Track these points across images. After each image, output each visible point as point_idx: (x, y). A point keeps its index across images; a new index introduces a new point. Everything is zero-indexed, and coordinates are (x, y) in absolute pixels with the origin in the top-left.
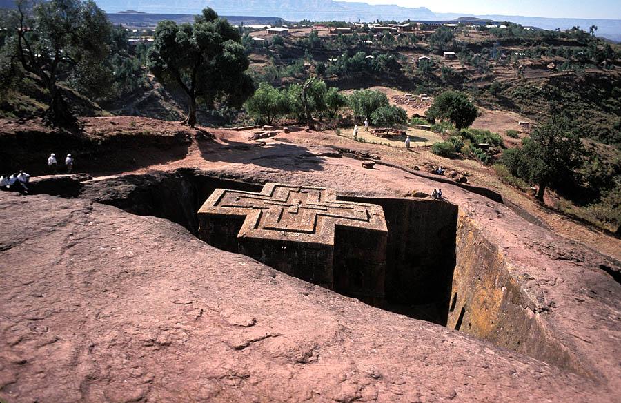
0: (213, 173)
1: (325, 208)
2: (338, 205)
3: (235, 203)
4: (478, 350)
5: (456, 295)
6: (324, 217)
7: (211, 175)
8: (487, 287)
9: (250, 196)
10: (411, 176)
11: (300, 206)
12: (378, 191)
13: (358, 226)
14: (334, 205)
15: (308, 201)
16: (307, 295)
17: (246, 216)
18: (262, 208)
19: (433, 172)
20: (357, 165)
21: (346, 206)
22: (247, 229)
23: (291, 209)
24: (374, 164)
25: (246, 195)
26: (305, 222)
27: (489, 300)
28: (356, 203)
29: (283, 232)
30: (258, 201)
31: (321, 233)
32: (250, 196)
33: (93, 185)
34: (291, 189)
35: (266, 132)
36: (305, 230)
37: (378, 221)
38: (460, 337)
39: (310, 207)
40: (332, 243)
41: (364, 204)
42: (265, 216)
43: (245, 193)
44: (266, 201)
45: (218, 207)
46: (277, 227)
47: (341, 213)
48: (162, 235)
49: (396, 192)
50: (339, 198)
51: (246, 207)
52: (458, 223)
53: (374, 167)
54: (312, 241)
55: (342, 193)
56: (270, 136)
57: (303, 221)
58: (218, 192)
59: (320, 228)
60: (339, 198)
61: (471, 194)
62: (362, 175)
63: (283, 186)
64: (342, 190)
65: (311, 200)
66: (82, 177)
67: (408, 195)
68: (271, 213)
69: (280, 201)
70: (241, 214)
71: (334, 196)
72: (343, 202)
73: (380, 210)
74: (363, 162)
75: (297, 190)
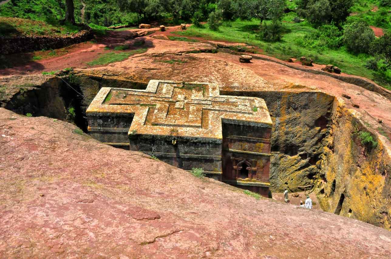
3: (121, 101)
4: (374, 237)
5: (335, 181)
8: (367, 174)
11: (186, 101)
12: (257, 85)
13: (244, 119)
14: (218, 100)
16: (204, 189)
17: (134, 113)
24: (251, 59)
25: (133, 93)
27: (369, 186)
28: (239, 97)
31: (210, 126)
34: (175, 85)
38: (355, 225)
39: (196, 102)
42: (153, 112)
45: (106, 106)
47: (226, 107)
50: (222, 93)
53: (251, 61)
54: (202, 135)
57: (190, 116)
59: (208, 122)
60: (222, 93)
62: (241, 70)
65: (196, 96)
70: (129, 111)
71: (217, 92)
73: (264, 104)
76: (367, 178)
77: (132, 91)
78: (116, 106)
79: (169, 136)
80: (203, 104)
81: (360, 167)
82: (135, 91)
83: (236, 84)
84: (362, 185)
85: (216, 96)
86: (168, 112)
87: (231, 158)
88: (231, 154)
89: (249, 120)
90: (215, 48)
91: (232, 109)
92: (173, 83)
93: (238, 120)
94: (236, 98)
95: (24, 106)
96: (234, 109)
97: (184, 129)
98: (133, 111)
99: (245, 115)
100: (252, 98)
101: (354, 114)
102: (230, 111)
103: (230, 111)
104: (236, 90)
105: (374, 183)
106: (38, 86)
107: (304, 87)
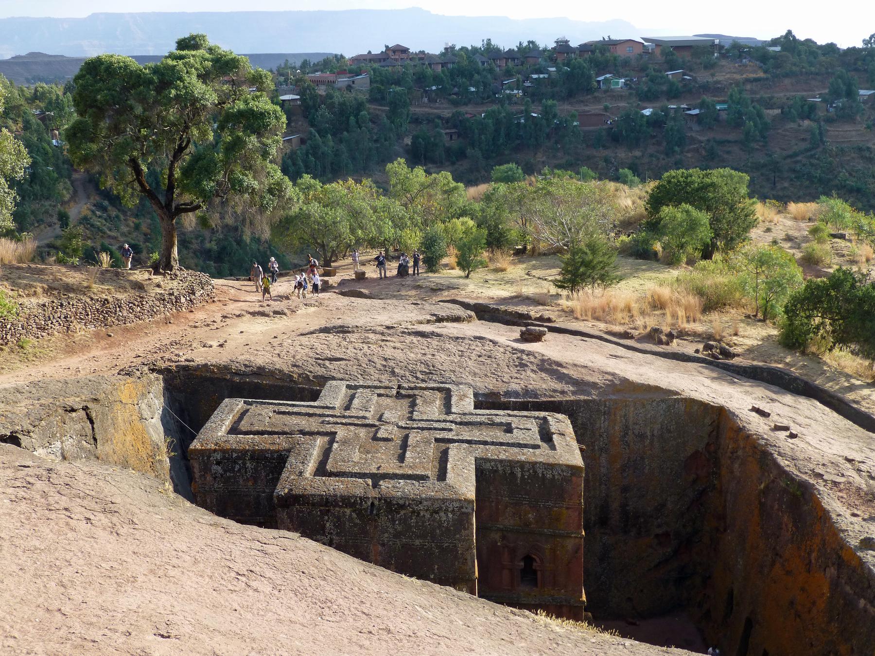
2: (478, 419)
10: (621, 351)
13: (523, 458)
14: (468, 418)
25: (290, 409)
28: (516, 413)
32: (296, 410)
34: (382, 391)
36: (410, 472)
40: (471, 495)
43: (287, 406)
44: (327, 419)
46: (356, 470)
69: (358, 418)
72: (488, 412)
77: (288, 405)
78: (252, 436)
79: (361, 498)
80: (435, 429)
81: (781, 557)
82: (293, 405)
85: (466, 411)
87: (499, 544)
88: (499, 534)
91: (497, 437)
93: (509, 461)
94: (509, 415)
95: (62, 443)
99: (525, 450)
100: (542, 414)
102: (493, 443)
103: (493, 443)
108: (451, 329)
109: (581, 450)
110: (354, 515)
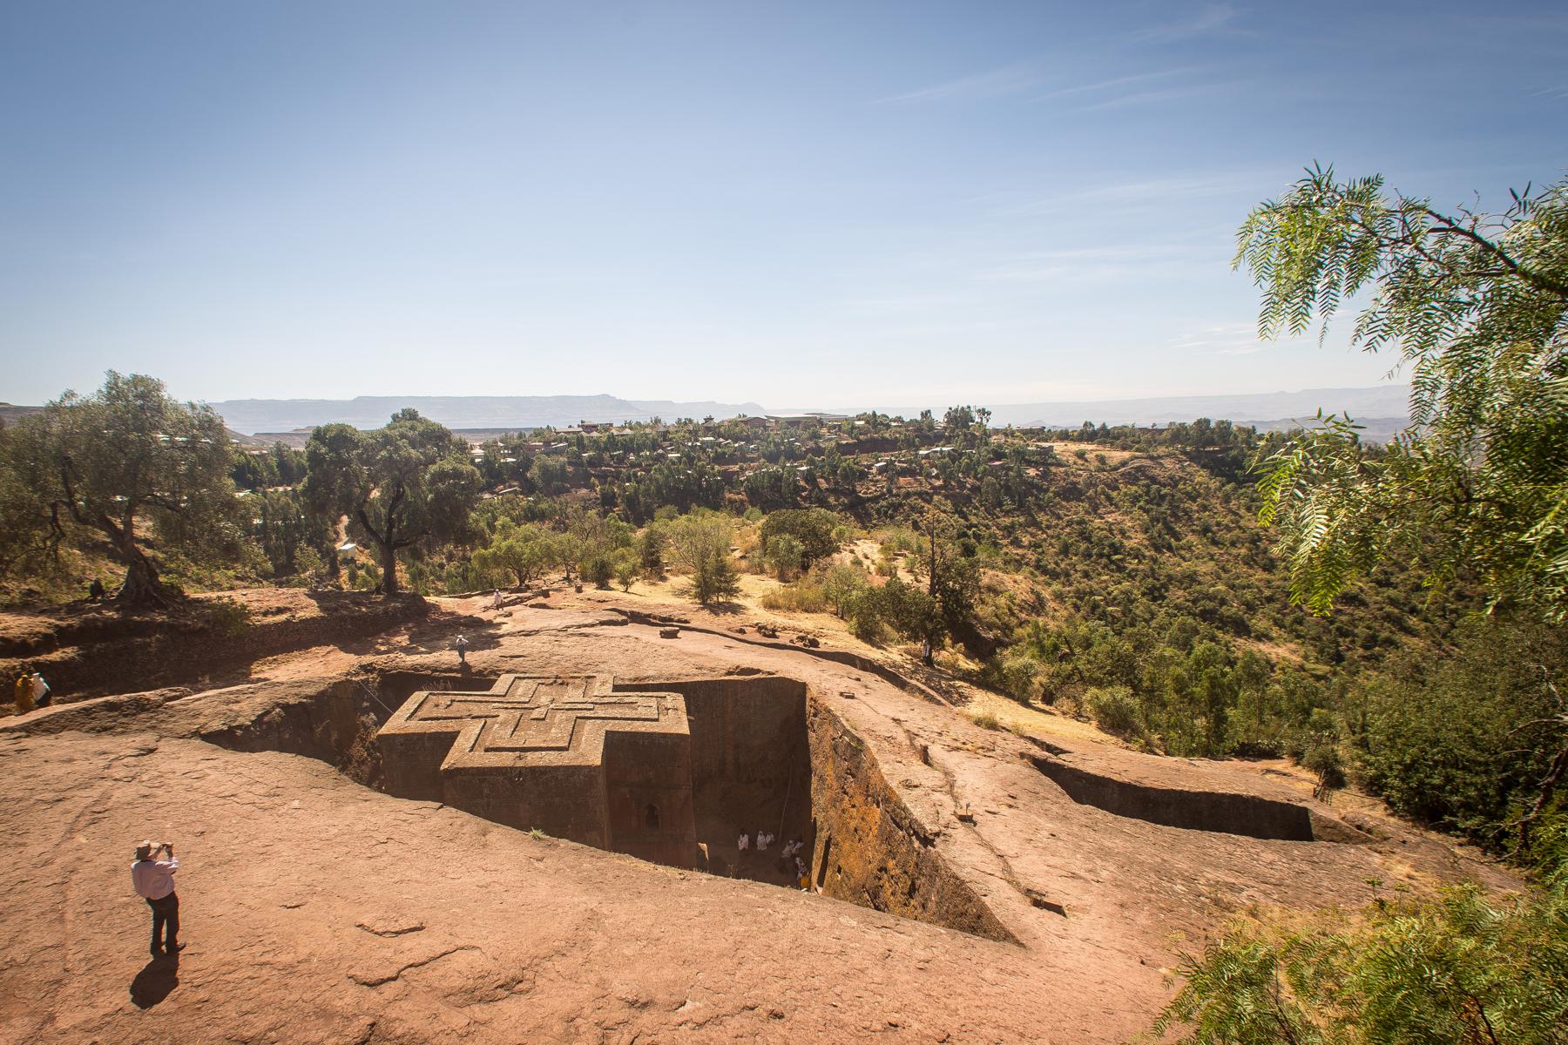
0: (414, 668)
1: (591, 706)
2: (613, 700)
6: (588, 722)
7: (416, 669)
9: (470, 698)
10: (733, 643)
11: (552, 706)
13: (643, 730)
15: (566, 699)
17: (459, 732)
18: (486, 717)
19: (765, 635)
20: (650, 635)
21: (627, 700)
22: (459, 756)
23: (535, 714)
24: (678, 631)
26: (557, 735)
28: (643, 694)
29: (518, 753)
30: (482, 705)
32: (470, 698)
33: (191, 706)
35: (514, 596)
36: (552, 745)
37: (675, 720)
39: (567, 707)
41: (655, 694)
43: (460, 695)
48: (280, 785)
49: (712, 670)
50: (616, 688)
51: (461, 718)
52: (808, 708)
54: (566, 762)
55: (630, 680)
56: (522, 602)
57: (553, 730)
58: (419, 696)
60: (616, 688)
61: (825, 663)
63: (528, 678)
64: (627, 674)
66: (174, 694)
67: (729, 673)
68: (501, 724)
70: (450, 730)
73: (681, 698)
74: (662, 629)
75: (551, 681)
76: (858, 811)
82: (468, 695)
83: (651, 673)
84: (853, 824)
86: (517, 725)
89: (651, 730)
90: (624, 618)
92: (539, 678)
96: (629, 713)
97: (538, 754)
98: (457, 729)
99: (646, 723)
100: (663, 694)
101: (832, 708)
104: (651, 682)
105: (868, 819)
106: (311, 697)
107: (758, 671)
108: (609, 630)
109: (689, 720)
110: (506, 781)
